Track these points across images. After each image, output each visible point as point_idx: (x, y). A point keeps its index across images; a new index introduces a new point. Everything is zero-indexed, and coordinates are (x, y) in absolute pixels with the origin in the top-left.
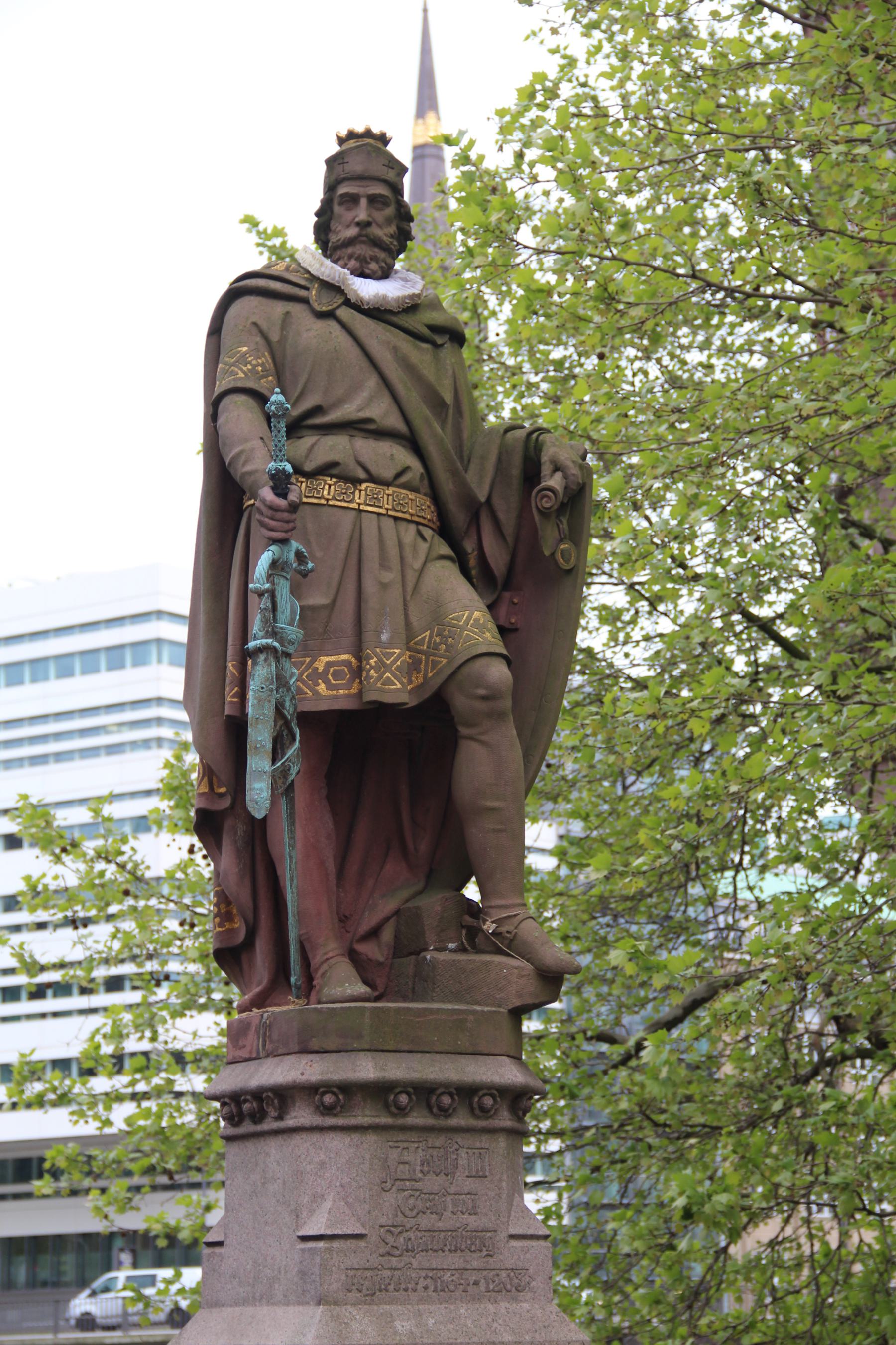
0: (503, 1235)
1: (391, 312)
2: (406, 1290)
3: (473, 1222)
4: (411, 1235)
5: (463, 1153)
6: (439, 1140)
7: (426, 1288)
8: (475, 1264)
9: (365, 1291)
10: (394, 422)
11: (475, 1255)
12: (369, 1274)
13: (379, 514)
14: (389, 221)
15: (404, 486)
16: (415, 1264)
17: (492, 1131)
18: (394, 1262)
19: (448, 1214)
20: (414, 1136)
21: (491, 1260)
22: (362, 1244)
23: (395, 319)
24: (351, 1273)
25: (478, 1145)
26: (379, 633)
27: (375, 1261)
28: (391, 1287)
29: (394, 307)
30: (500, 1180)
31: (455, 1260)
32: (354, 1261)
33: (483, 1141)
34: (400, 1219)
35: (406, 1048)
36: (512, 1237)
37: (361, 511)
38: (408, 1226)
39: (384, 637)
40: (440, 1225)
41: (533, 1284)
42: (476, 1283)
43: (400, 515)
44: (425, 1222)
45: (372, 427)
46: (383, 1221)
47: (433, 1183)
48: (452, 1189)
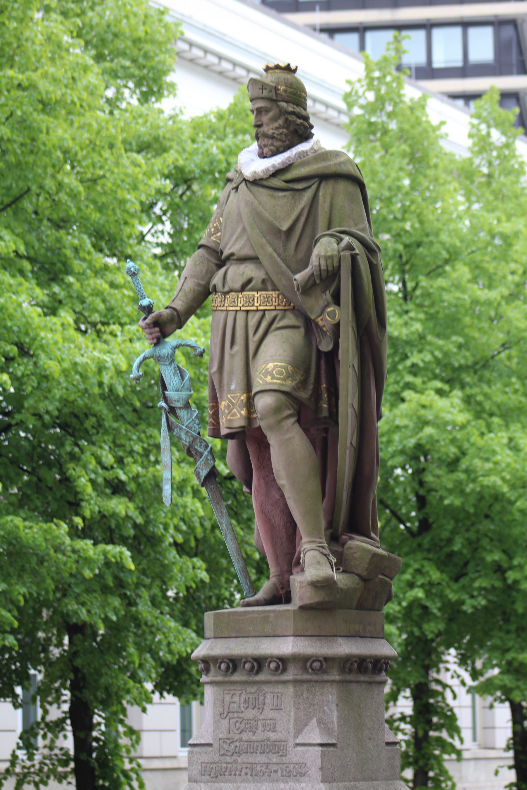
0: (291, 743)
1: (261, 179)
2: (235, 775)
3: (273, 736)
4: (238, 744)
5: (269, 696)
6: (253, 689)
7: (246, 774)
8: (274, 761)
9: (212, 775)
10: (247, 251)
11: (275, 755)
12: (214, 766)
13: (237, 311)
14: (274, 119)
15: (252, 290)
16: (239, 760)
17: (285, 682)
18: (228, 759)
19: (259, 731)
20: (239, 687)
21: (284, 758)
22: (210, 749)
23: (265, 183)
24: (204, 765)
25: (276, 690)
26: (229, 385)
27: (217, 758)
28: (227, 773)
30: (290, 711)
31: (261, 758)
32: (206, 759)
33: (280, 689)
34: (231, 735)
35: (234, 635)
36: (298, 745)
37: (227, 311)
38: (235, 739)
39: (233, 387)
40: (254, 738)
41: (310, 772)
42: (276, 771)
43: (248, 308)
44: (245, 736)
45: (235, 257)
46: (221, 736)
47: (250, 714)
48: (261, 717)
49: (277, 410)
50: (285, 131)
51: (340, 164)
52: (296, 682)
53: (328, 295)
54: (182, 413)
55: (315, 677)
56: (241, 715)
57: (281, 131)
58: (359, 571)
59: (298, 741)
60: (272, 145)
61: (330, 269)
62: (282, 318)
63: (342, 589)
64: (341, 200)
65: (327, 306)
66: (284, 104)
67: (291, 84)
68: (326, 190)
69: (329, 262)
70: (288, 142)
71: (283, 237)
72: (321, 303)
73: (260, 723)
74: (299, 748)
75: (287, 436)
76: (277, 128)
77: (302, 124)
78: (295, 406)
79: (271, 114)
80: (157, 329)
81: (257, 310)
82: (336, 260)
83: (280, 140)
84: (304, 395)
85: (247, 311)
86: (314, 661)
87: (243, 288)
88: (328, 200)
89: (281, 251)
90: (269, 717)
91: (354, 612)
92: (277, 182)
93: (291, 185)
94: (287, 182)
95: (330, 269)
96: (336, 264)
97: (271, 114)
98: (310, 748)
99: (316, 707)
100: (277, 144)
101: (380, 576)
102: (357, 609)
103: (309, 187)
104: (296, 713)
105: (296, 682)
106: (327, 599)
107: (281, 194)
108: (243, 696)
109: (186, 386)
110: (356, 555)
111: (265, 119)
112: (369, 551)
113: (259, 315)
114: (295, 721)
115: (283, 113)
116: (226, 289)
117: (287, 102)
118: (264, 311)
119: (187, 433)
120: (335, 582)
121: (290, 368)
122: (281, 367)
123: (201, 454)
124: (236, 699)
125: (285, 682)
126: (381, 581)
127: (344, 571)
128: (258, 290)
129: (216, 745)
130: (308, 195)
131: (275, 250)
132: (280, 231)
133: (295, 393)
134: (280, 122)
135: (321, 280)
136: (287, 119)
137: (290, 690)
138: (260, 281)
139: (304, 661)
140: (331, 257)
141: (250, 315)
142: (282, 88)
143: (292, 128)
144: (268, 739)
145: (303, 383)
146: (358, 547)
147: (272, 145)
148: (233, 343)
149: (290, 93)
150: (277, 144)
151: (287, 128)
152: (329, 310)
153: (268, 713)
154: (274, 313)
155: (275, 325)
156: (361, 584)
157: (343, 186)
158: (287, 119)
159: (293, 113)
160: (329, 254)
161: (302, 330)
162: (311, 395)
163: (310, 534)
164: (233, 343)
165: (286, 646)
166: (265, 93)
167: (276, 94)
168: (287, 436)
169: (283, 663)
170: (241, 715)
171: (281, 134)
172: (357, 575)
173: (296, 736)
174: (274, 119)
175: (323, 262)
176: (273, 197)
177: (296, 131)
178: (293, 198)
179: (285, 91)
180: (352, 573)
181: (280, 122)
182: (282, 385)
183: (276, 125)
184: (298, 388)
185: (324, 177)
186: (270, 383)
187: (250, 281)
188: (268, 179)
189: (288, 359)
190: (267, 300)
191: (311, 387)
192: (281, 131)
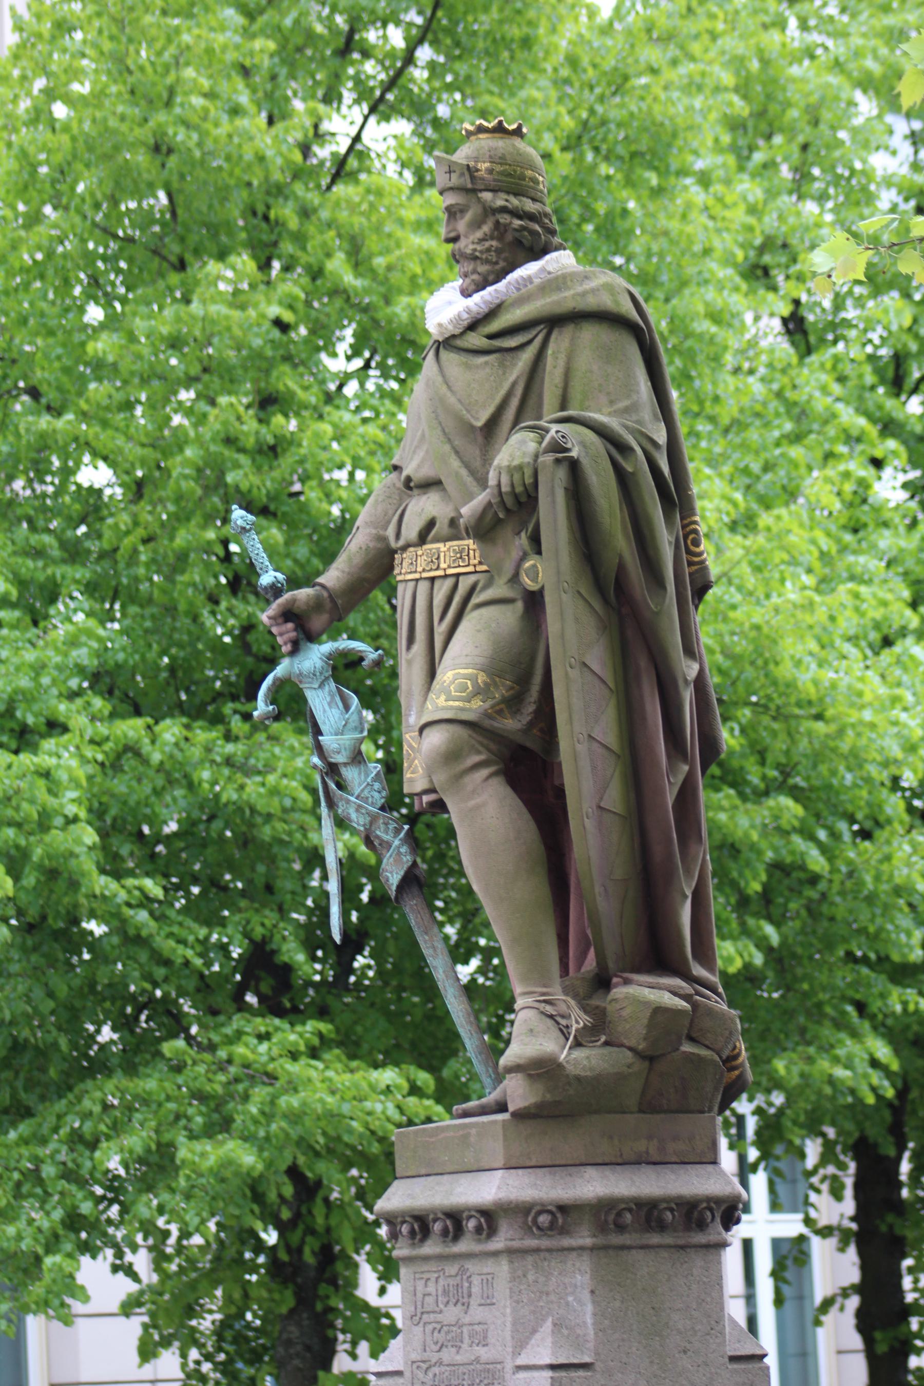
0: (509, 1366)
3: (484, 1353)
4: (436, 1370)
5: (476, 1280)
6: (452, 1269)
14: (476, 224)
15: (437, 540)
17: (495, 1254)
19: (465, 1346)
20: (433, 1266)
22: (399, 1380)
29: (452, 330)
33: (489, 1266)
34: (425, 1356)
36: (520, 1368)
40: (459, 1358)
47: (451, 1314)
48: (467, 1320)
49: (451, 756)
50: (494, 243)
51: (584, 294)
52: (511, 1253)
53: (523, 540)
54: (350, 774)
55: (545, 1243)
56: (439, 1317)
57: (487, 244)
58: (632, 1043)
59: (520, 1361)
60: (474, 271)
61: (519, 489)
62: (486, 587)
63: (578, 1079)
64: (586, 360)
65: (523, 558)
66: (487, 196)
67: (503, 157)
68: (560, 343)
69: (517, 477)
70: (502, 264)
71: (480, 439)
72: (515, 554)
73: (465, 1330)
74: (522, 1375)
75: (471, 803)
76: (481, 241)
77: (523, 228)
78: (492, 746)
79: (468, 216)
80: (290, 625)
81: (446, 576)
82: (528, 473)
83: (487, 261)
84: (511, 724)
85: (432, 580)
86: (540, 1213)
87: (423, 538)
88: (561, 363)
89: (477, 463)
90: (477, 1319)
91: (631, 1119)
92: (475, 340)
93: (497, 343)
94: (491, 337)
95: (519, 489)
96: (529, 480)
97: (468, 216)
98: (536, 1374)
99: (552, 1297)
100: (483, 268)
101: (687, 1048)
102: (641, 1111)
103: (530, 342)
104: (514, 1310)
105: (511, 1253)
106: (548, 1097)
107: (482, 359)
108: (441, 1282)
109: (352, 724)
110: (624, 1013)
111: (461, 226)
112: (647, 1003)
113: (449, 582)
114: (514, 1324)
115: (489, 211)
116: (401, 543)
117: (493, 191)
118: (458, 575)
119: (359, 808)
120: (560, 1066)
121: (482, 678)
122: (466, 677)
123: (389, 845)
124: (431, 1288)
125: (495, 1254)
126: (689, 1057)
127: (606, 1043)
128: (445, 540)
129: (407, 1374)
130: (527, 355)
131: (467, 465)
132: (472, 427)
133: (487, 723)
134: (486, 228)
135: (508, 511)
136: (497, 223)
137: (503, 1268)
138: (446, 522)
139: (523, 1213)
140: (520, 468)
141: (437, 584)
142: (484, 166)
143: (509, 237)
144: (477, 1360)
145: (513, 703)
146: (627, 997)
147: (474, 271)
148: (411, 640)
149: (501, 173)
150: (483, 268)
151: (500, 238)
152: (527, 565)
153: (477, 1313)
154: (472, 579)
155: (475, 600)
156: (640, 1066)
157: (589, 334)
158: (497, 223)
159: (504, 210)
160: (516, 463)
161: (520, 605)
162: (531, 724)
163: (525, 979)
164: (411, 640)
165: (486, 1189)
166: (455, 180)
167: (473, 178)
168: (471, 803)
169: (489, 1218)
170: (439, 1317)
171: (488, 250)
172: (630, 1049)
173: (516, 1353)
174: (476, 224)
175: (505, 480)
176: (468, 367)
177: (518, 243)
178: (502, 365)
179: (490, 171)
180: (621, 1045)
181: (486, 228)
182: (462, 709)
183: (479, 234)
184: (500, 712)
185: (554, 322)
186: (444, 708)
187: (431, 524)
188: (462, 334)
189: (479, 660)
190: (461, 554)
191: (530, 708)
192: (487, 244)
